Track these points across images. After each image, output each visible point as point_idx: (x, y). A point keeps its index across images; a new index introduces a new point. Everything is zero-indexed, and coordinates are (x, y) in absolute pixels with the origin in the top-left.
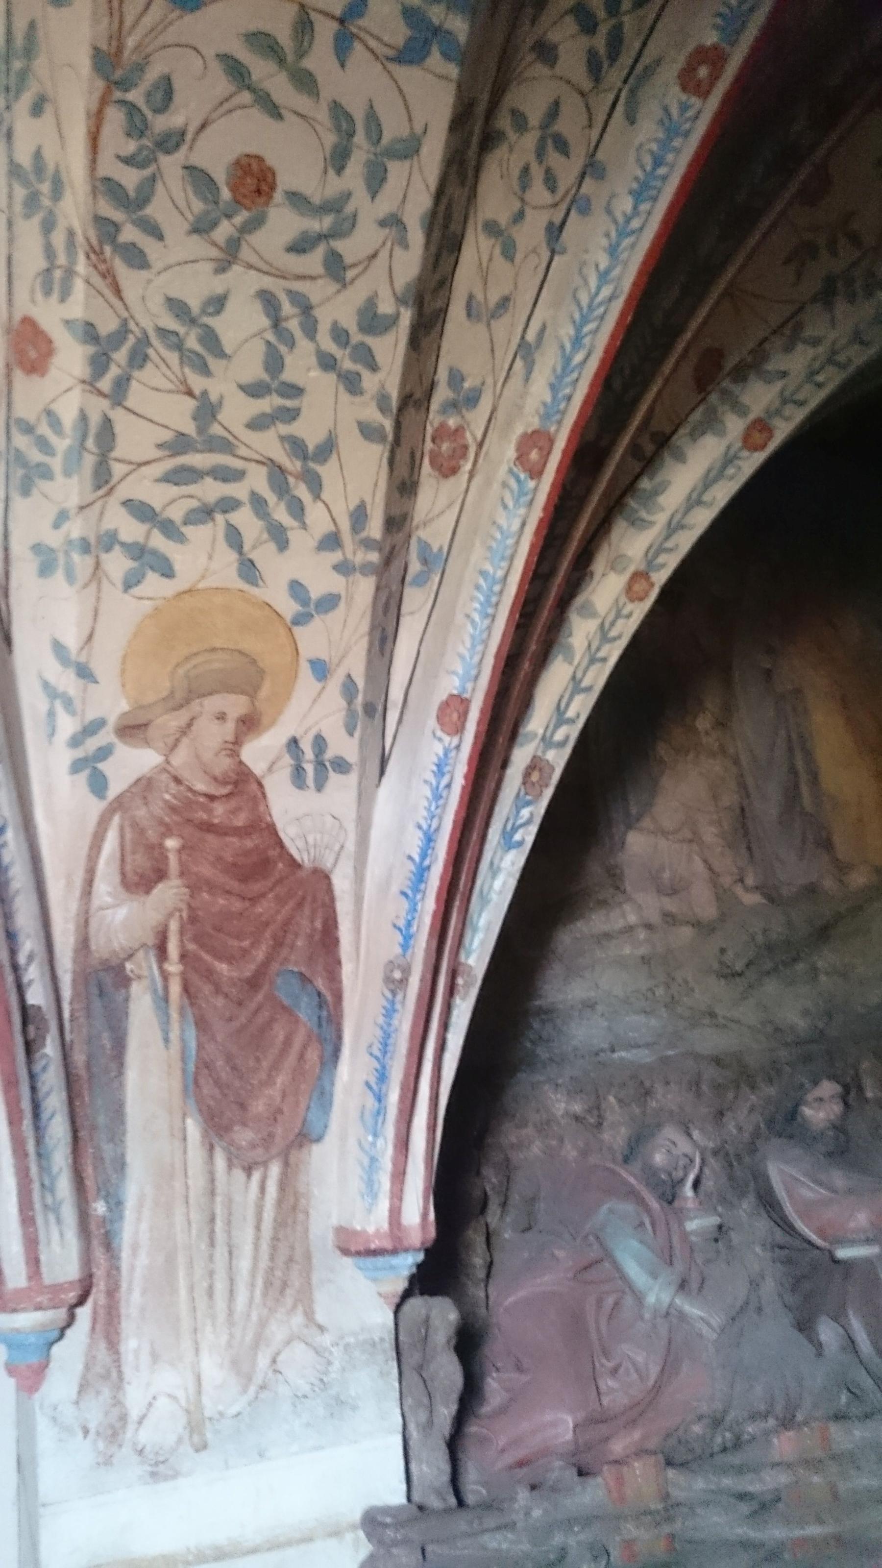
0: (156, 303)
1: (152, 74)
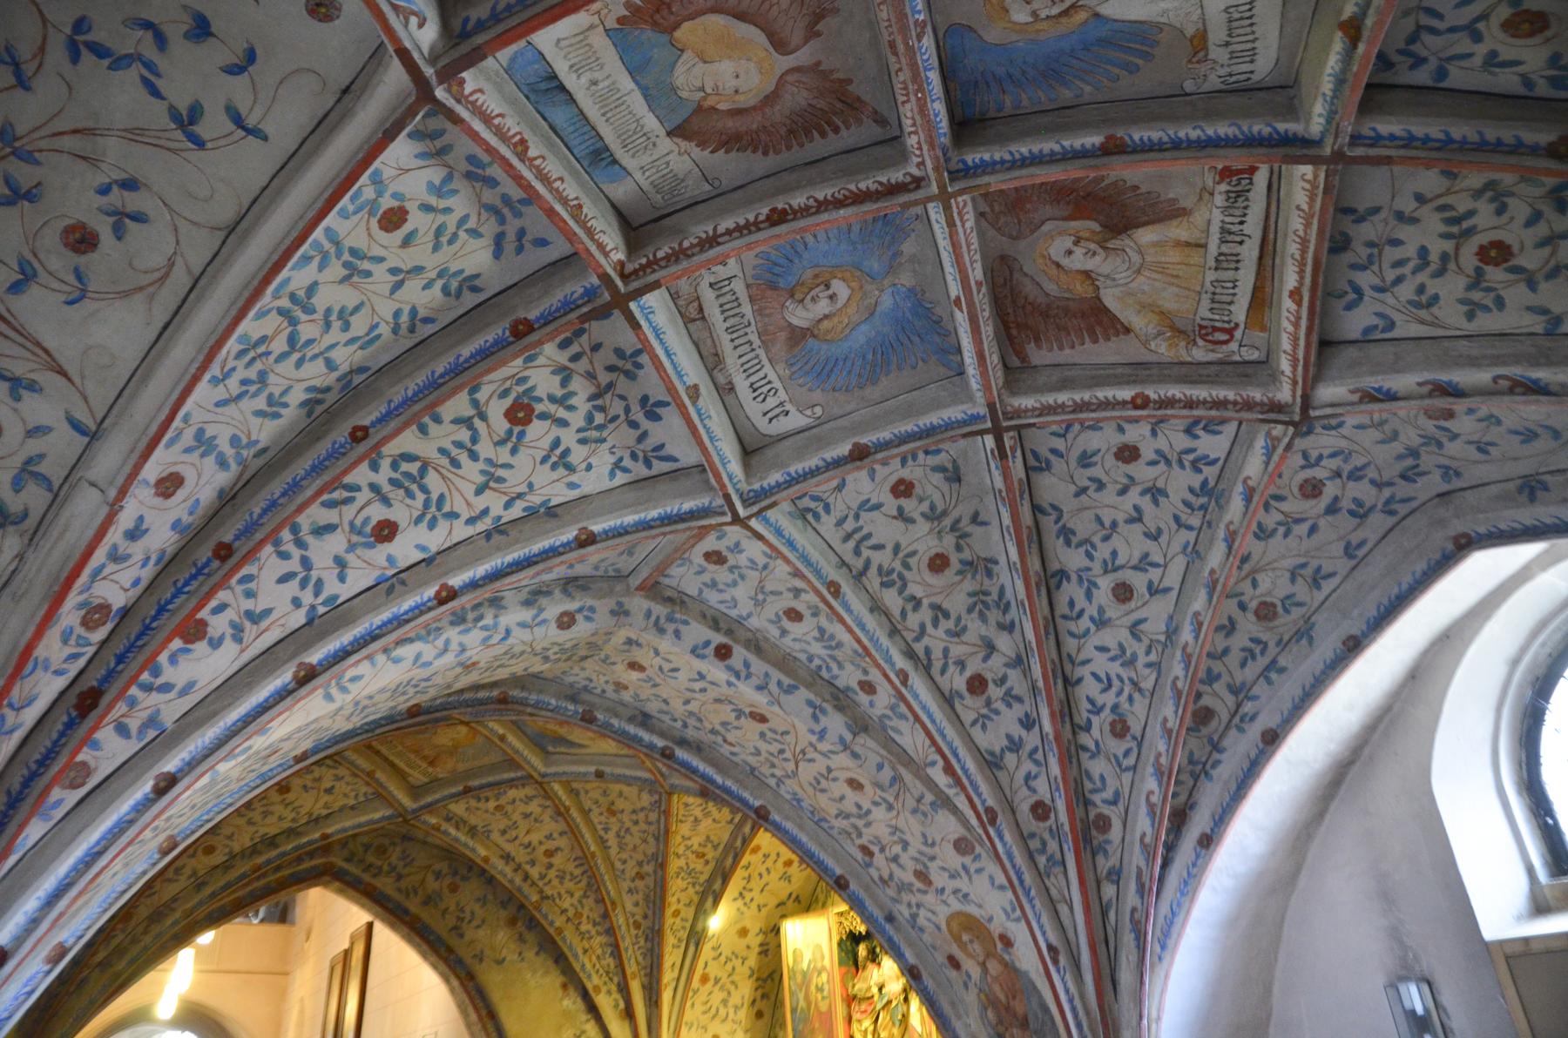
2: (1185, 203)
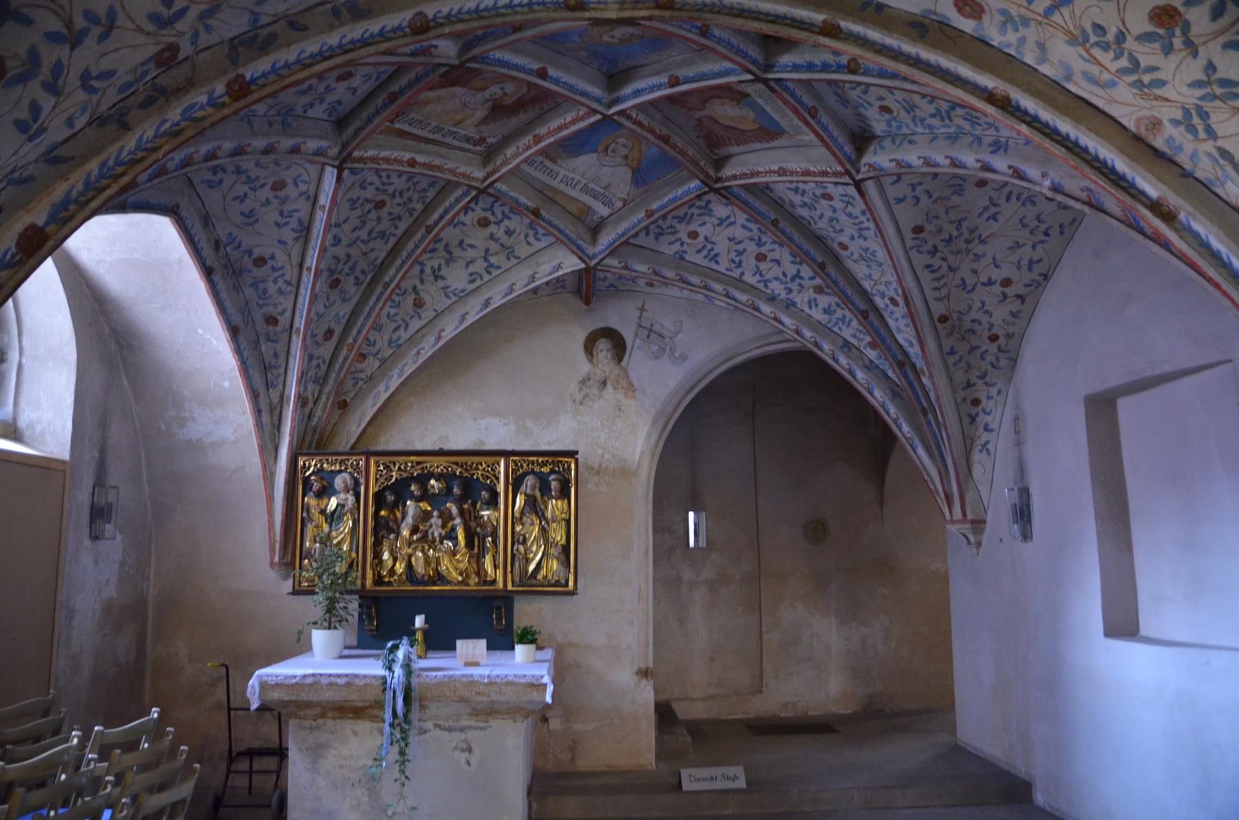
0: (1185, 90)
1: (1088, 27)
2: (482, 128)
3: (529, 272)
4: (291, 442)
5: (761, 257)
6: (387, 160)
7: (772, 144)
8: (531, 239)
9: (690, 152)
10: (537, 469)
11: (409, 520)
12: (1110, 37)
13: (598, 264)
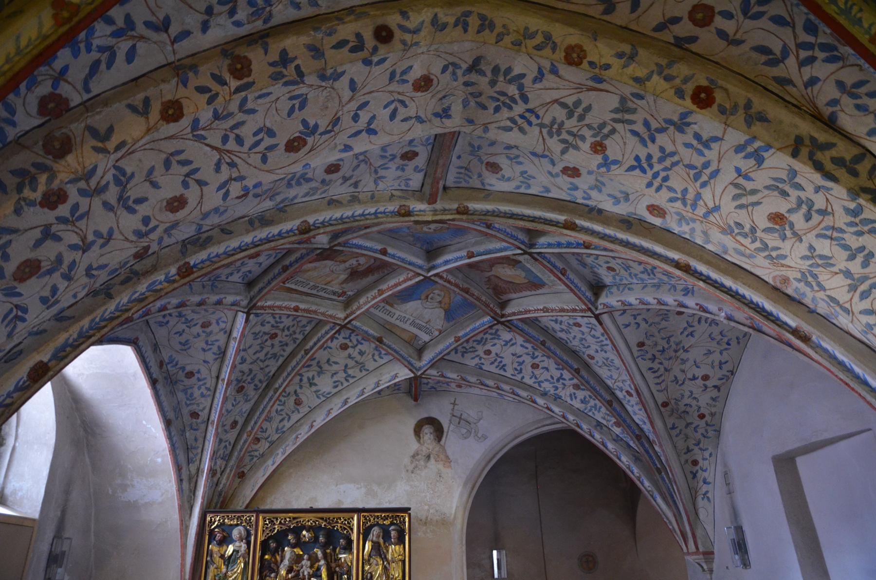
0: (799, 261)
1: (732, 224)
2: (344, 286)
3: (376, 380)
4: (202, 503)
5: (535, 366)
6: (280, 308)
7: (540, 291)
8: (377, 357)
9: (483, 298)
10: (381, 522)
11: (286, 562)
12: (747, 228)
13: (422, 374)
